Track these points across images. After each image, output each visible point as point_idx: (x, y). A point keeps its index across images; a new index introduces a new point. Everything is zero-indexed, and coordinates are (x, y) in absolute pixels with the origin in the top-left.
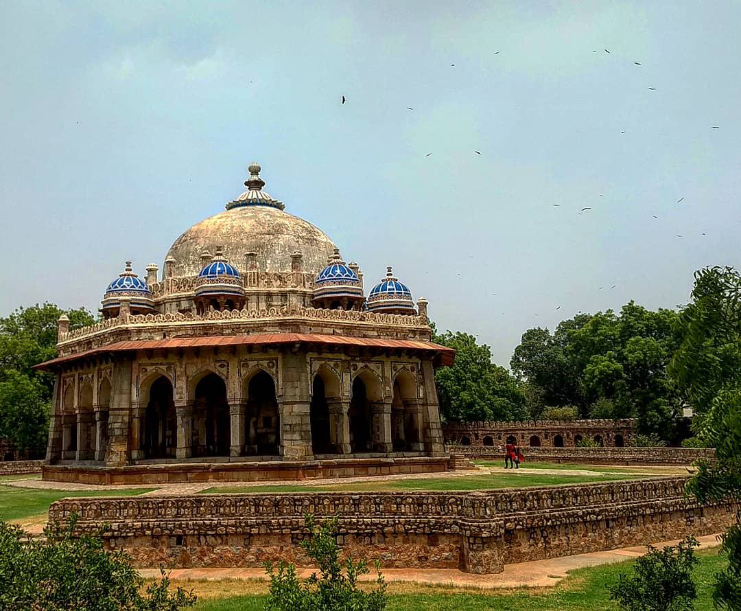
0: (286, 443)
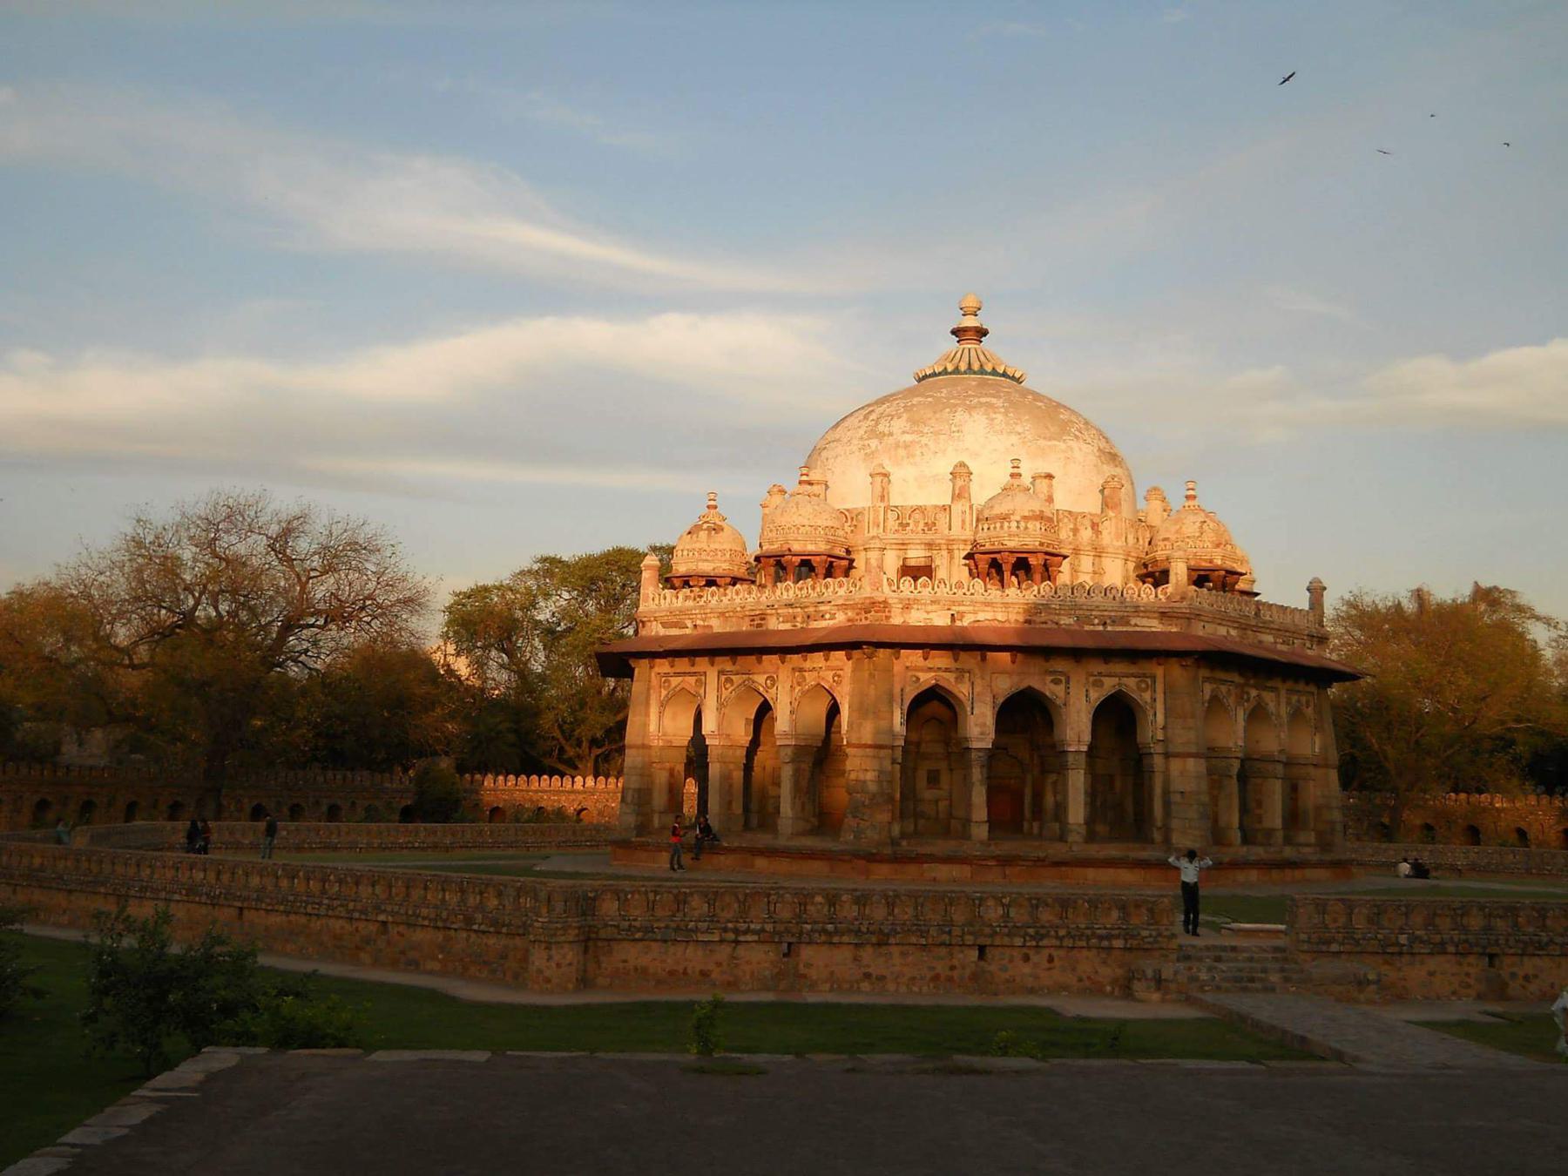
0: (1175, 824)
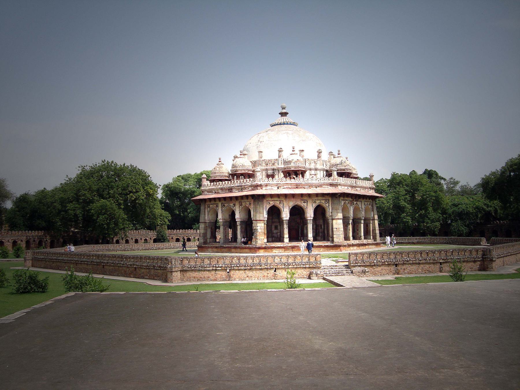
0: (335, 236)
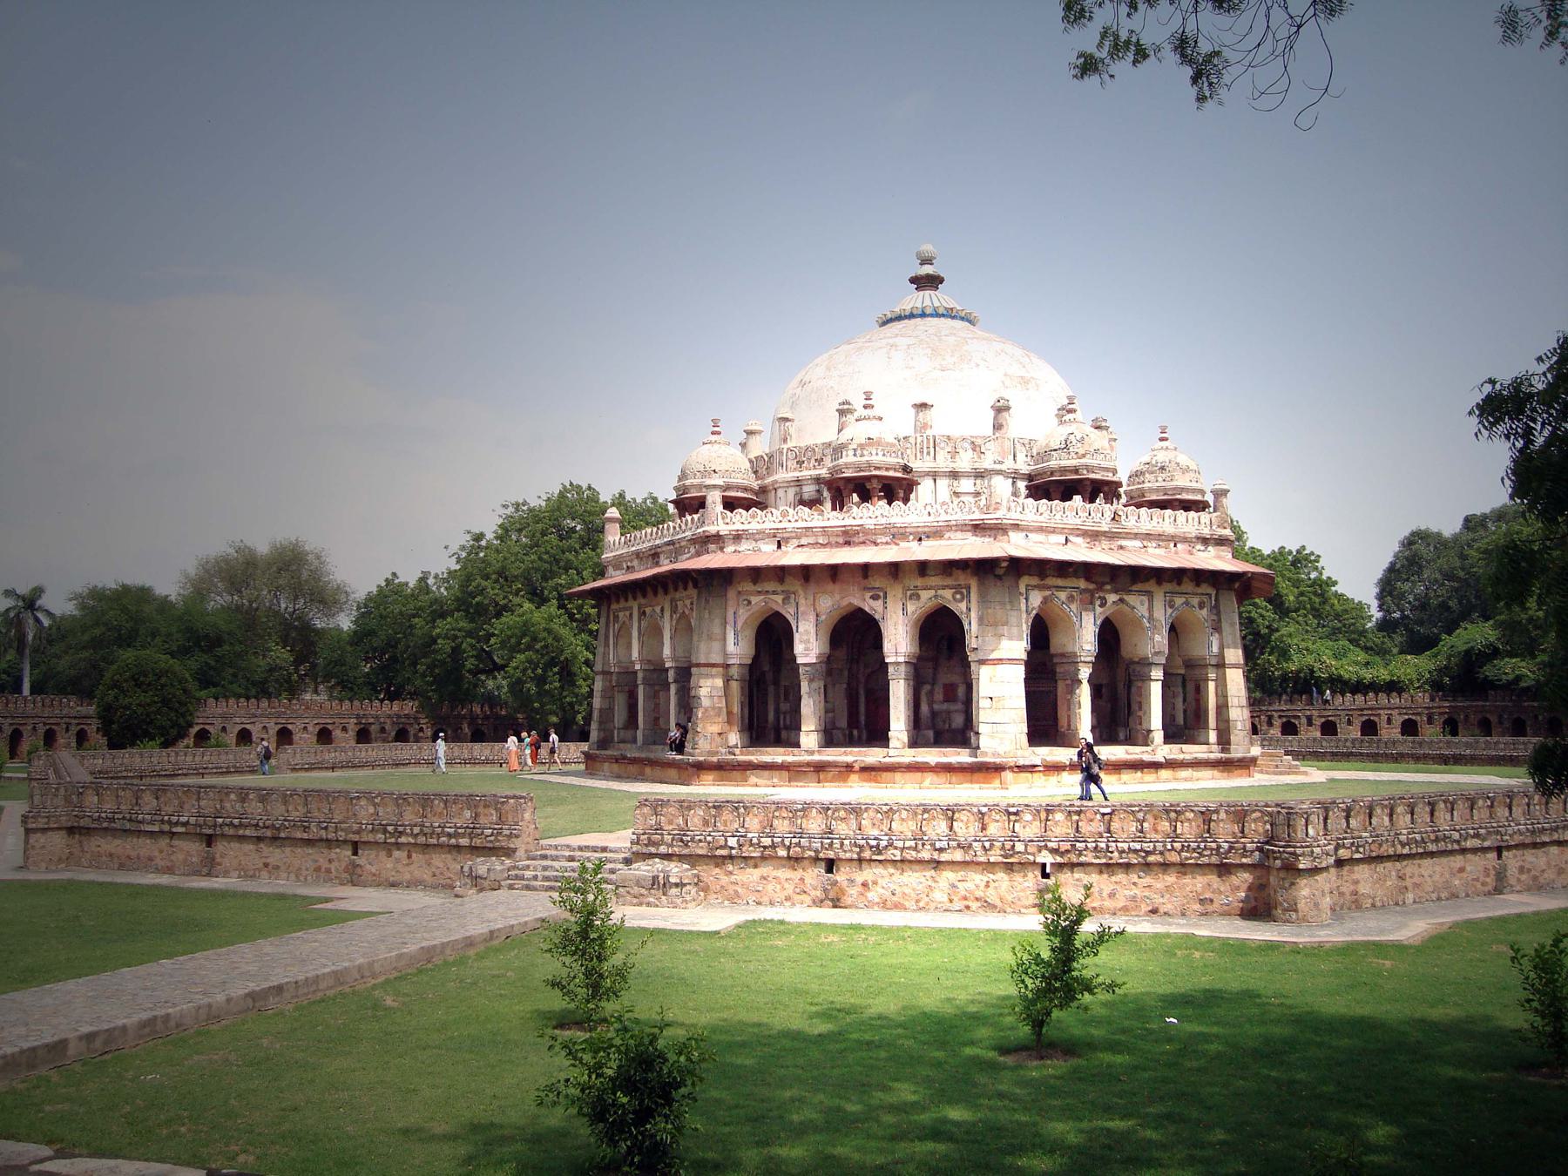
0: (982, 729)
